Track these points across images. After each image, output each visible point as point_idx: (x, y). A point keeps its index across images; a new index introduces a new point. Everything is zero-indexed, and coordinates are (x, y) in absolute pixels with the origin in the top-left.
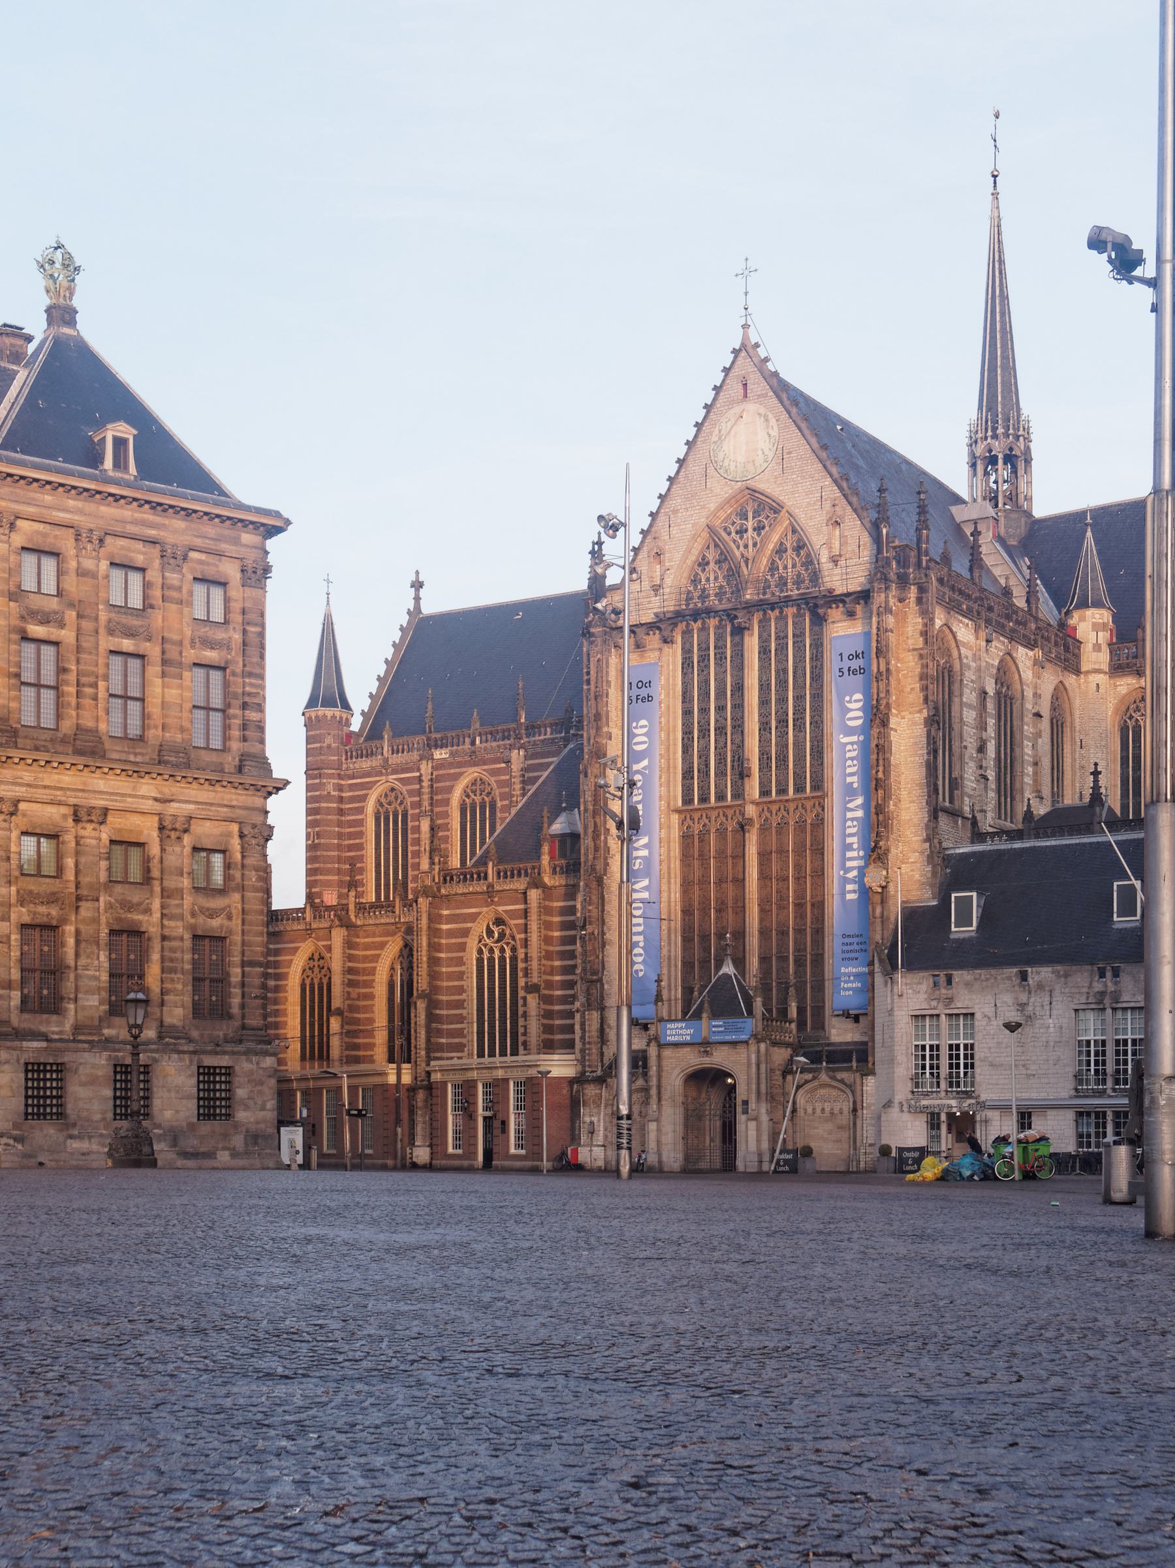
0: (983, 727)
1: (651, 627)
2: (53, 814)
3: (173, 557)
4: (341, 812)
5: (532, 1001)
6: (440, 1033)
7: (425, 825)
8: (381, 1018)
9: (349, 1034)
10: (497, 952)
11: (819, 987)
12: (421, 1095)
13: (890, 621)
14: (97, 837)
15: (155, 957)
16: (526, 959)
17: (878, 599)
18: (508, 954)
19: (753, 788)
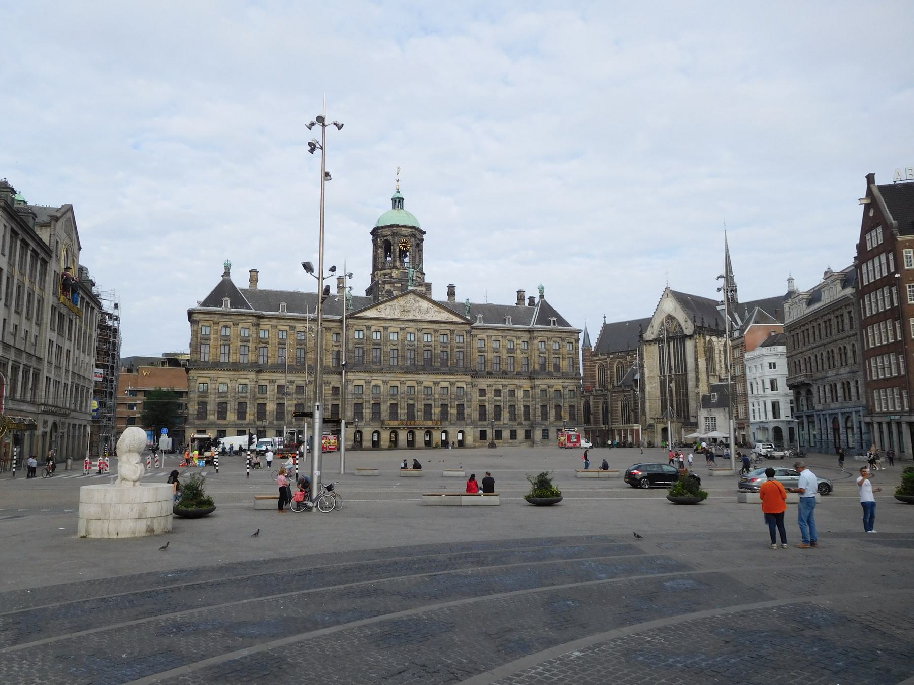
0: (720, 357)
1: (651, 341)
2: (545, 387)
3: (563, 340)
4: (590, 369)
5: (632, 413)
6: (614, 419)
7: (609, 372)
8: (601, 416)
9: (595, 418)
11: (688, 411)
12: (610, 432)
13: (697, 341)
14: (552, 390)
17: (695, 337)
19: (673, 372)
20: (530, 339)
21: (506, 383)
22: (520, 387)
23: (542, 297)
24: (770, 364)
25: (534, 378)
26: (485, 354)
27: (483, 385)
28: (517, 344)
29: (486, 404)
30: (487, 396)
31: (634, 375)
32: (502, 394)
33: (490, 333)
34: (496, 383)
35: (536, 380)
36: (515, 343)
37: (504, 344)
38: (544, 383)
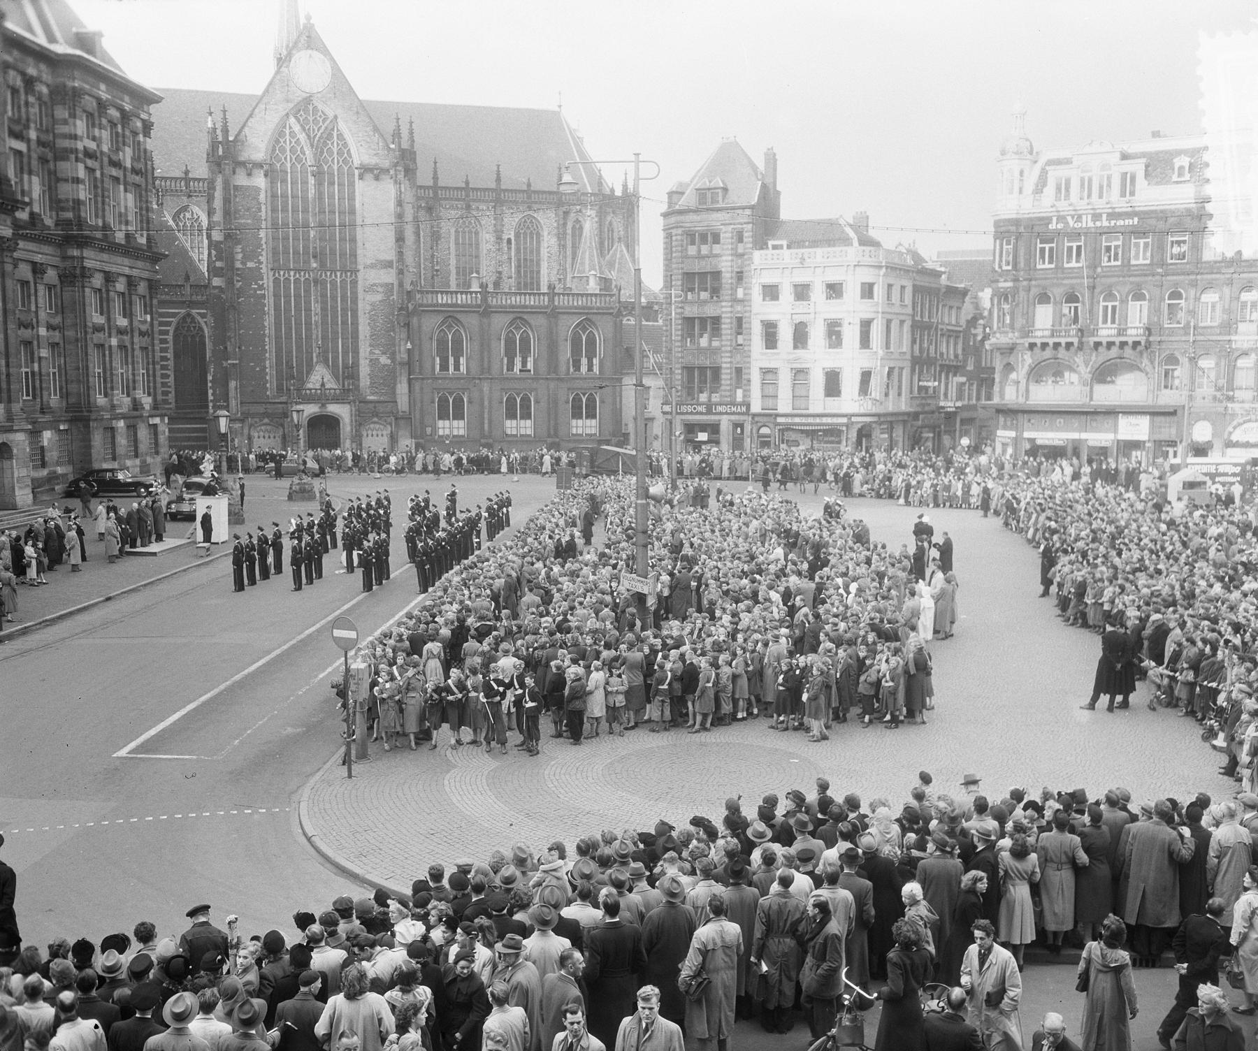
36: (23, 97)
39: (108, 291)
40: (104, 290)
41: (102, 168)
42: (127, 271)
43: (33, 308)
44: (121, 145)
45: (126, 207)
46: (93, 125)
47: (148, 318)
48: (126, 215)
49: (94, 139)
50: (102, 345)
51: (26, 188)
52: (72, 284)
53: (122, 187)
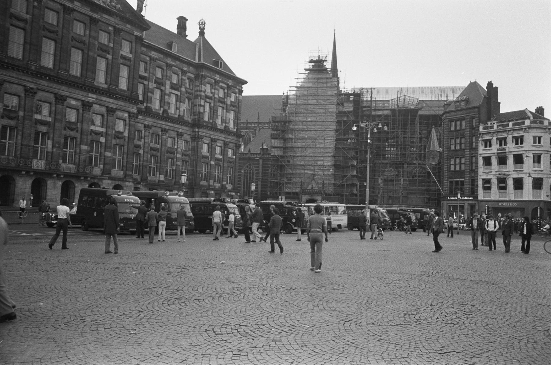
10: (249, 172)
15: (222, 171)
16: (258, 173)
18: (251, 171)
20: (197, 77)
21: (167, 128)
22: (180, 135)
23: (202, 33)
24: (535, 137)
25: (198, 128)
26: (146, 83)
27: (140, 125)
28: (182, 79)
29: (141, 152)
30: (143, 140)
31: (263, 144)
32: (160, 141)
33: (154, 54)
34: (155, 125)
35: (200, 130)
36: (180, 77)
37: (168, 74)
38: (207, 135)
39: (212, 145)
40: (210, 144)
41: (214, 103)
42: (223, 139)
43: (176, 147)
44: (226, 96)
45: (226, 117)
46: (212, 89)
47: (234, 157)
48: (226, 120)
49: (212, 93)
50: (208, 164)
51: (178, 106)
52: (194, 141)
53: (225, 111)
